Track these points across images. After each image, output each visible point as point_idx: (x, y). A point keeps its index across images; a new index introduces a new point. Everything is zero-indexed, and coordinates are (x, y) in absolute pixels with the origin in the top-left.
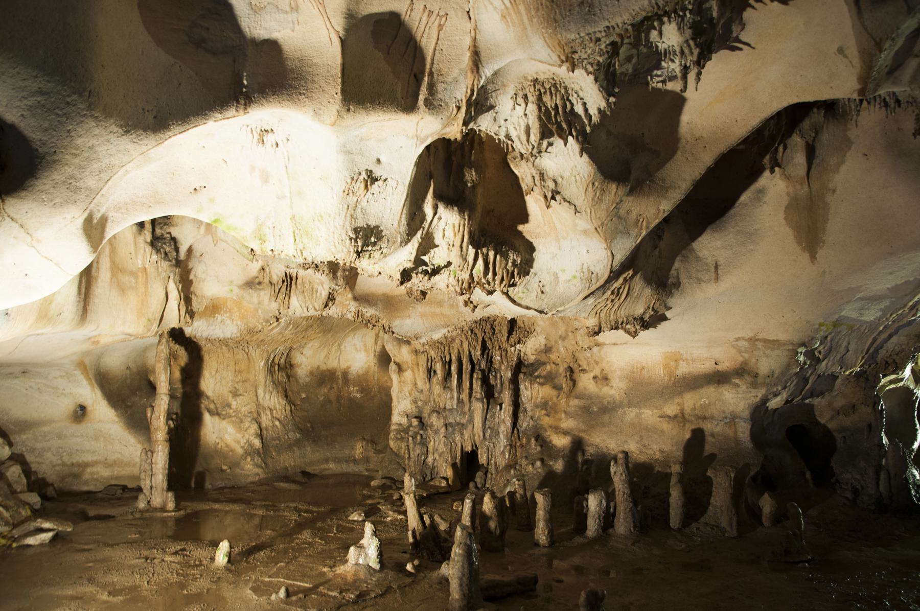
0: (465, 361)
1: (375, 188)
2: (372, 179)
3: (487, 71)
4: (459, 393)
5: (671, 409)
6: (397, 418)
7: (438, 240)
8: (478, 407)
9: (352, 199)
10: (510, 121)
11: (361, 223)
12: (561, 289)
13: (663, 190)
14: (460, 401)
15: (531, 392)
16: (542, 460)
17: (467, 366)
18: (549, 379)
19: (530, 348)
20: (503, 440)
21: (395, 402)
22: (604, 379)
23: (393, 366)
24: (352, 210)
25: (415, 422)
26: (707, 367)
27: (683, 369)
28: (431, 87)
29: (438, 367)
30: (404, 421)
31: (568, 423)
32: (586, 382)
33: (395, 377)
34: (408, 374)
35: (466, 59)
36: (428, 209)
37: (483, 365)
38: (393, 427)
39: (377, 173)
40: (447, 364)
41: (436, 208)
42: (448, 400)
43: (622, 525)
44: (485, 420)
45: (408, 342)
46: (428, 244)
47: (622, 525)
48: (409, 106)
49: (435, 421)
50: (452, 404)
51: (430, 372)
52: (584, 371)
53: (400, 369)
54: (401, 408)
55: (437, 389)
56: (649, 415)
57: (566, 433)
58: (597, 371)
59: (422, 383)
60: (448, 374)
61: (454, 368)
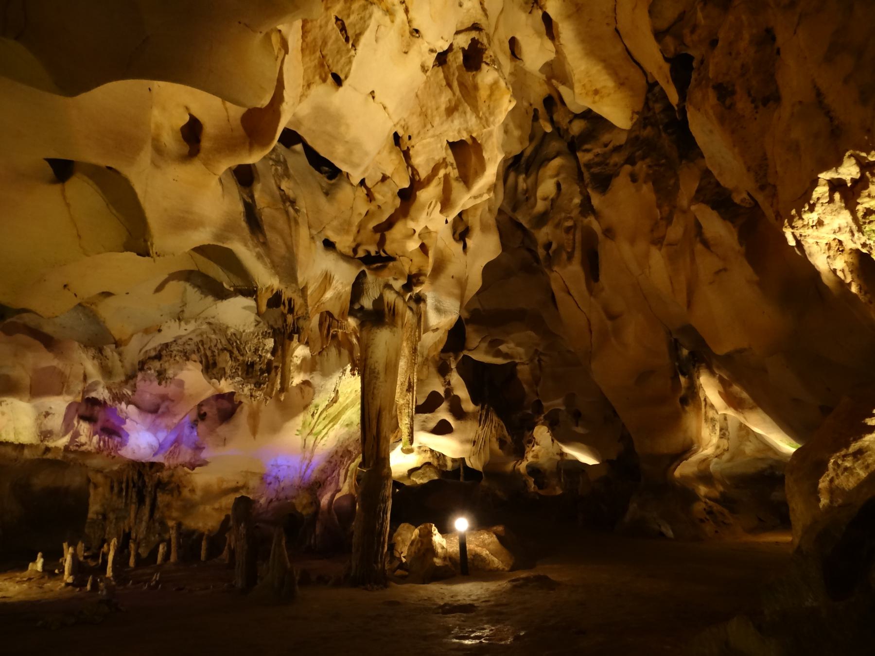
0: (130, 481)
1: (50, 417)
2: (47, 414)
3: (90, 381)
4: (126, 499)
5: (217, 506)
6: (91, 515)
7: (82, 432)
8: (133, 508)
9: (39, 422)
10: (102, 393)
11: (44, 429)
12: (142, 451)
13: (175, 415)
14: (126, 505)
15: (162, 499)
16: (159, 534)
17: (131, 485)
18: (171, 492)
19: (164, 475)
20: (144, 524)
21: (91, 506)
22: (193, 491)
23: (91, 485)
24: (39, 426)
25: (100, 517)
26: (233, 484)
27: (225, 486)
28: (68, 387)
29: (115, 485)
30: (95, 517)
31: (175, 514)
32: (186, 493)
33: (92, 491)
34: (100, 490)
35: (82, 377)
36: (75, 422)
37: (140, 484)
38: (88, 521)
39: (50, 411)
40: (120, 483)
41: (78, 423)
42: (120, 503)
43: (173, 558)
44: (137, 514)
45: (102, 472)
46: (77, 434)
47: (173, 558)
48: (59, 394)
49: (112, 516)
50: (122, 506)
51: (112, 488)
52: (185, 487)
53: (96, 486)
54: (94, 508)
55: (115, 498)
56: (208, 508)
57: (174, 519)
58: (190, 488)
59: (108, 495)
60: (121, 490)
61: (124, 486)
